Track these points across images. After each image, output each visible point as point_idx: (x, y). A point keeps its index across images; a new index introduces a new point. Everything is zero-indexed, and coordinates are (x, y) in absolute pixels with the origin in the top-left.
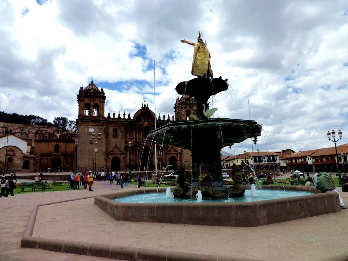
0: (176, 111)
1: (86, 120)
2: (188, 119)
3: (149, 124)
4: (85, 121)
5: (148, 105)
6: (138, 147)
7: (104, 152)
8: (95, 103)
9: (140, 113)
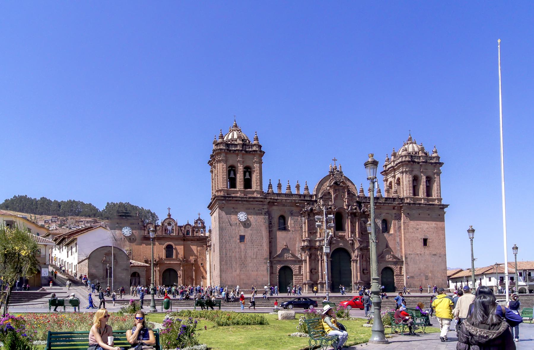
1: (233, 197)
4: (230, 200)
8: (245, 165)
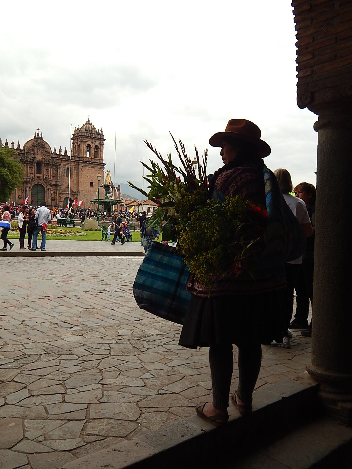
0: (73, 143)
2: (88, 156)
3: (43, 159)
5: (41, 135)
6: (30, 183)
9: (31, 143)
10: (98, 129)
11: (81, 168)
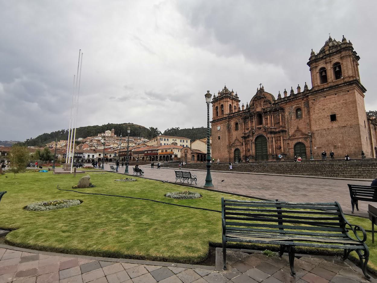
7: (227, 145)
8: (221, 105)
10: (339, 40)
11: (312, 103)
